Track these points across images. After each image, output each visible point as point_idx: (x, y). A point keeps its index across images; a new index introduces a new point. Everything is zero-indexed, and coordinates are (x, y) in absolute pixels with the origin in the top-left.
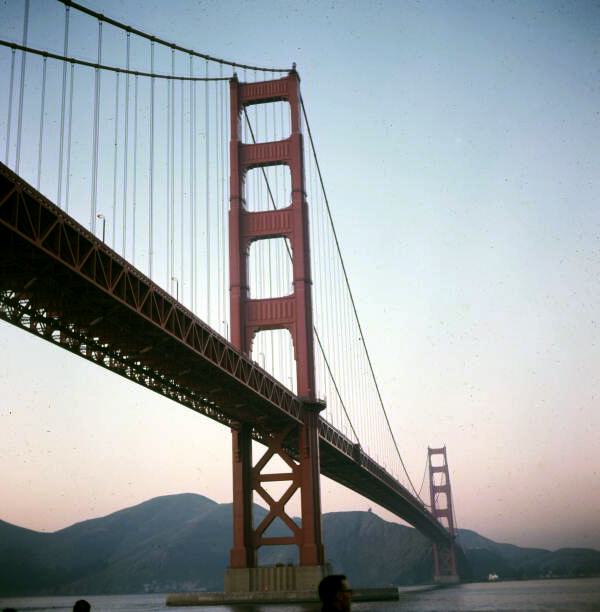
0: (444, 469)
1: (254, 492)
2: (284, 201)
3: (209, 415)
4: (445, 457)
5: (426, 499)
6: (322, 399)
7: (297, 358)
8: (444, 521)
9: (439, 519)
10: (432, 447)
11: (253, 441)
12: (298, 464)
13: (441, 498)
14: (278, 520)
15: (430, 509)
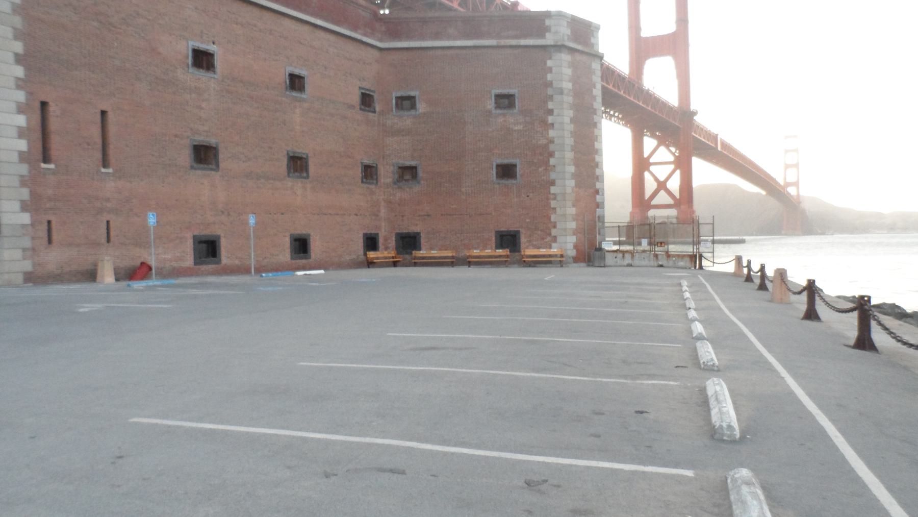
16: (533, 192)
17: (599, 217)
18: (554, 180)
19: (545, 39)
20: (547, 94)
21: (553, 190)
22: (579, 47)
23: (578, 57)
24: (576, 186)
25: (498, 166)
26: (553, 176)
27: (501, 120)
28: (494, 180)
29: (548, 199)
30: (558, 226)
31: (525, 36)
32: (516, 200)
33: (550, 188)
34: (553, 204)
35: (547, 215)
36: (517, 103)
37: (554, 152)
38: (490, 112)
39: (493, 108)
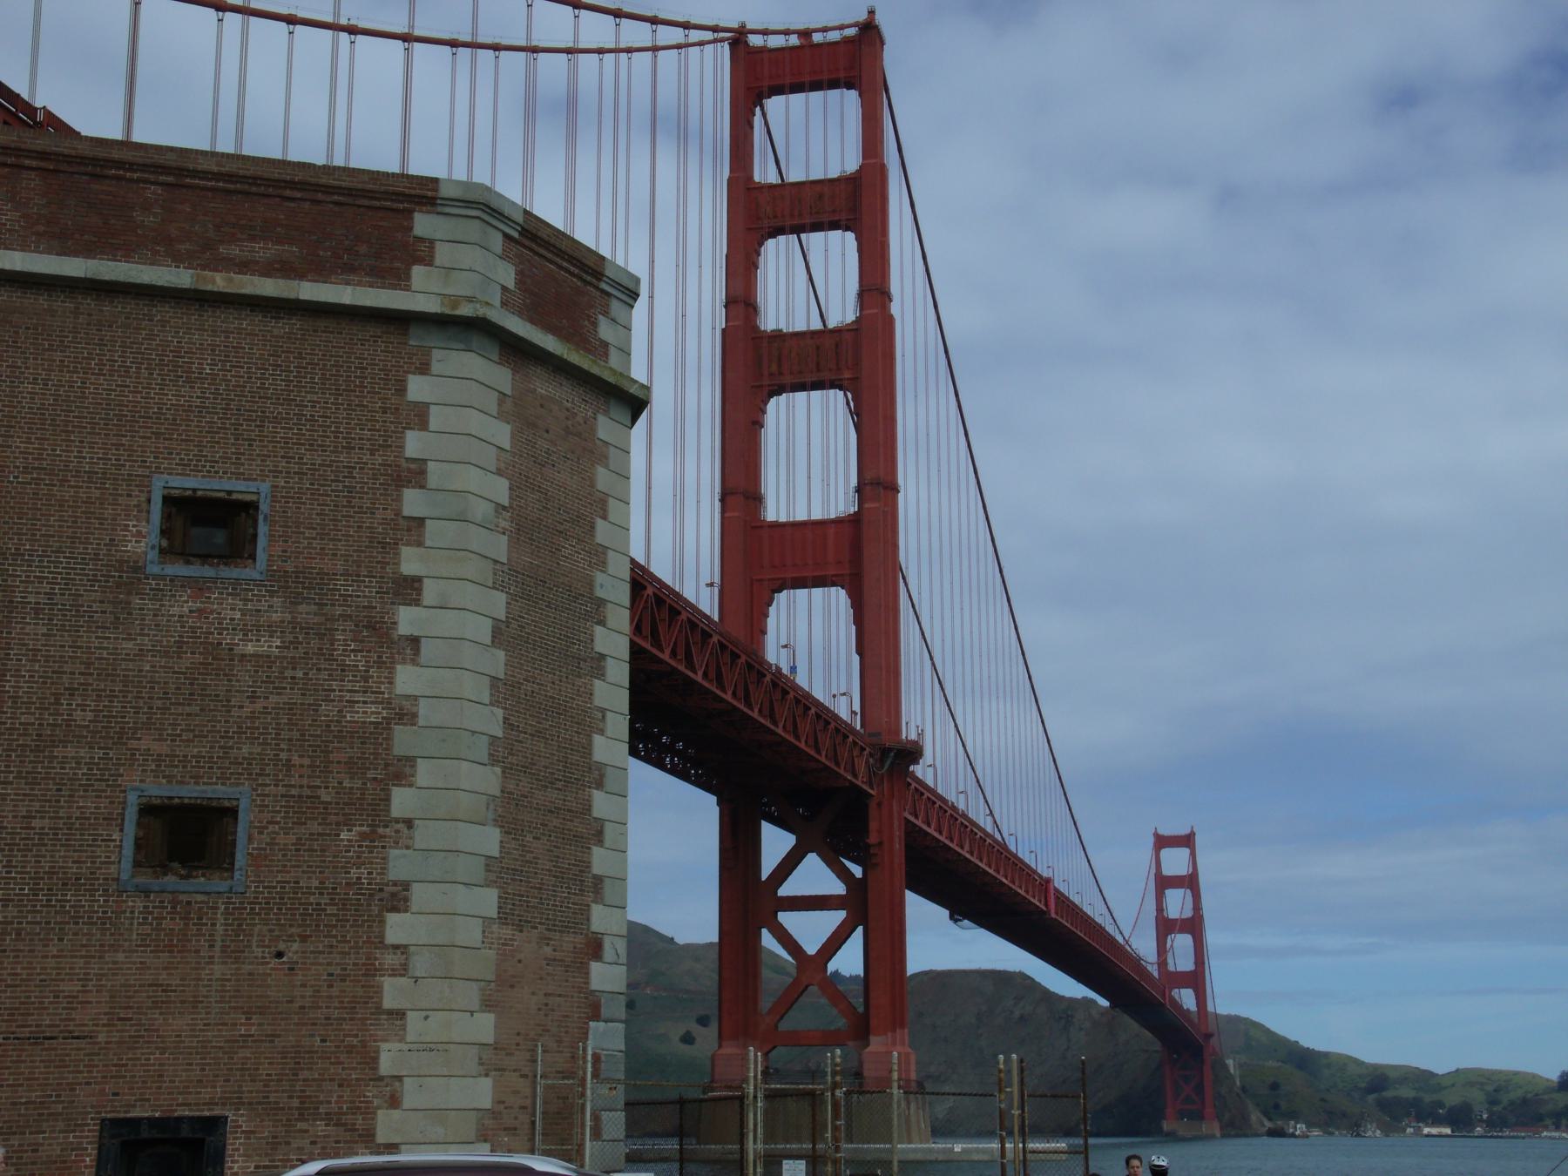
0: (1190, 882)
1: (765, 931)
2: (842, 310)
3: (673, 772)
4: (1193, 855)
5: (1144, 945)
6: (913, 736)
7: (860, 651)
8: (1187, 998)
9: (1175, 992)
10: (1165, 831)
11: (764, 823)
12: (857, 871)
13: (1181, 947)
14: (814, 996)
15: (1154, 971)
16: (304, 938)
17: (597, 1058)
18: (406, 886)
19: (408, 288)
20: (398, 513)
21: (397, 928)
22: (548, 342)
23: (544, 386)
24: (504, 917)
25: (149, 810)
26: (399, 865)
27: (182, 605)
28: (125, 876)
29: (371, 971)
30: (412, 1095)
31: (320, 271)
32: (218, 970)
33: (382, 922)
34: (392, 992)
35: (364, 1044)
36: (262, 542)
37: (411, 761)
38: (137, 568)
39: (153, 555)
